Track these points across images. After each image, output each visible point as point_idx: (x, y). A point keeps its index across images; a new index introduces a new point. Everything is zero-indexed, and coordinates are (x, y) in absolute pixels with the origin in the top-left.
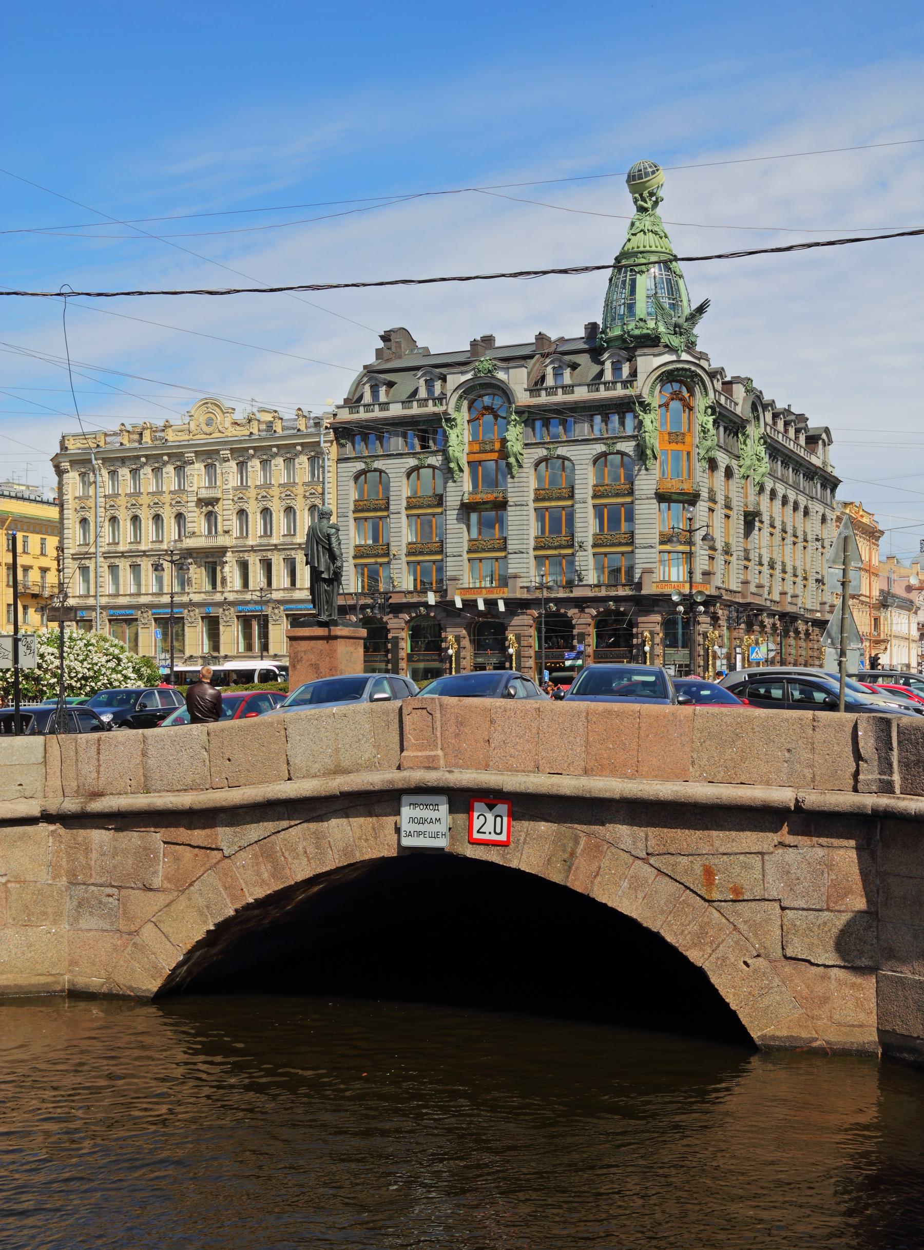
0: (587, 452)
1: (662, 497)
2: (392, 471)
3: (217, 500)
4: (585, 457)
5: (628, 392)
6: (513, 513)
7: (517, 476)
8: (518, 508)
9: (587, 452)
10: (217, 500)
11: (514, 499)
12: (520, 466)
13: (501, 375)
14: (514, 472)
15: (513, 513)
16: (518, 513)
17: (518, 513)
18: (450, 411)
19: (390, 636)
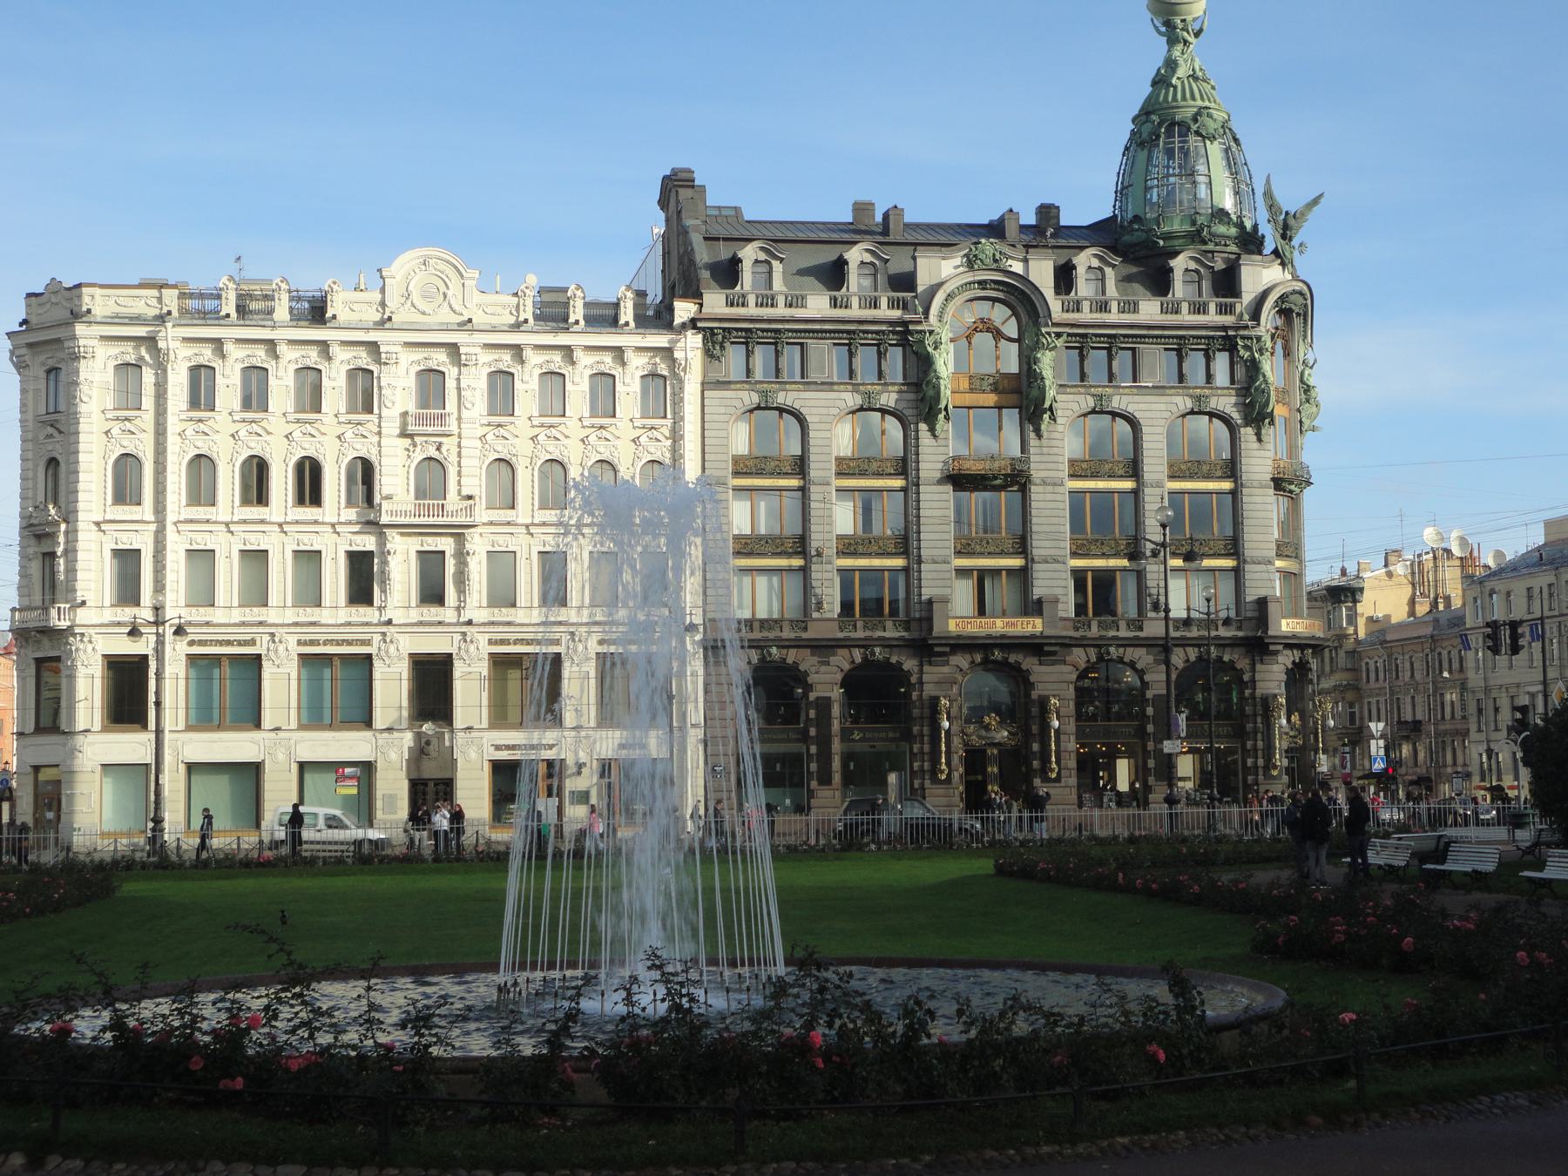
0: (1163, 407)
1: (960, 480)
2: (814, 411)
4: (1158, 415)
5: (1228, 320)
6: (1040, 497)
7: (1045, 434)
8: (1050, 488)
9: (1163, 407)
11: (1043, 474)
12: (1053, 418)
13: (1017, 267)
14: (1043, 427)
15: (1040, 497)
16: (1049, 497)
17: (1049, 497)
19: (812, 696)
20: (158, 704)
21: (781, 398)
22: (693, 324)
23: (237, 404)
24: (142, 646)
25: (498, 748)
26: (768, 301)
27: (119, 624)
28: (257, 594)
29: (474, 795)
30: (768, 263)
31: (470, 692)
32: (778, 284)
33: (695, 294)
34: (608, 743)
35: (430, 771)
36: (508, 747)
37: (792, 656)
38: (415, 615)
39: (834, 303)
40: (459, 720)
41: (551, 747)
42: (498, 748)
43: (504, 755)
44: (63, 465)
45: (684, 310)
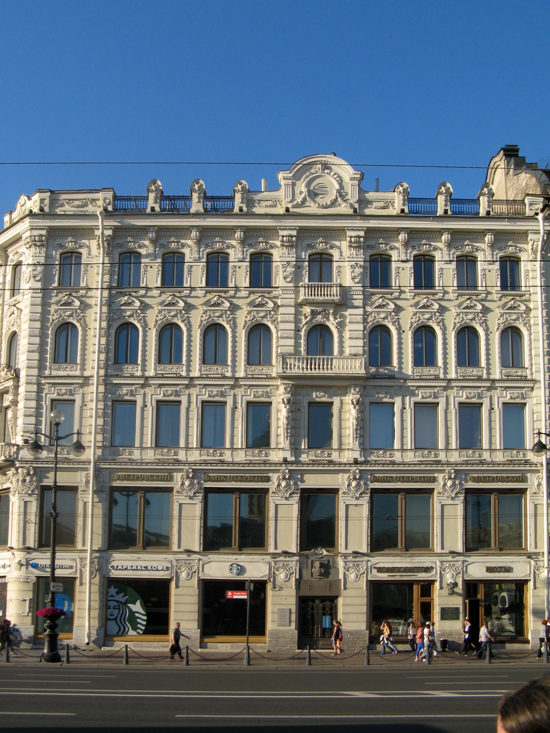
25: (380, 570)
29: (352, 612)
35: (318, 589)
41: (427, 570)
42: (380, 570)
43: (384, 576)
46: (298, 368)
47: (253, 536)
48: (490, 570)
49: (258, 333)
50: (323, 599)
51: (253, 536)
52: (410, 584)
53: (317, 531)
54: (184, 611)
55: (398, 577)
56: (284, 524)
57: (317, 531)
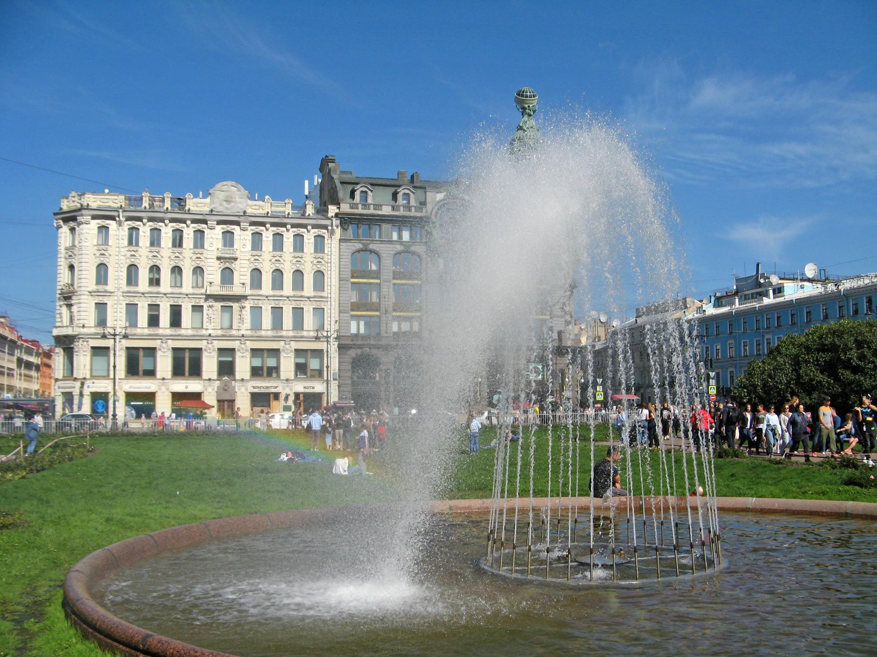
3: (236, 259)
10: (236, 259)
18: (433, 217)
20: (115, 367)
21: (371, 247)
22: (337, 215)
23: (148, 244)
24: (109, 343)
25: (254, 388)
26: (366, 205)
27: (98, 334)
28: (278, 323)
30: (366, 192)
31: (243, 365)
32: (370, 201)
33: (337, 203)
34: (300, 387)
35: (226, 397)
36: (258, 387)
37: (374, 351)
38: (220, 332)
39: (393, 208)
40: (238, 376)
41: (276, 387)
42: (254, 388)
44: (76, 269)
45: (332, 210)
46: (216, 290)
47: (196, 371)
48: (305, 388)
49: (198, 271)
50: (228, 401)
51: (196, 371)
52: (268, 394)
53: (226, 369)
54: (164, 406)
55: (263, 391)
56: (210, 365)
57: (226, 369)
